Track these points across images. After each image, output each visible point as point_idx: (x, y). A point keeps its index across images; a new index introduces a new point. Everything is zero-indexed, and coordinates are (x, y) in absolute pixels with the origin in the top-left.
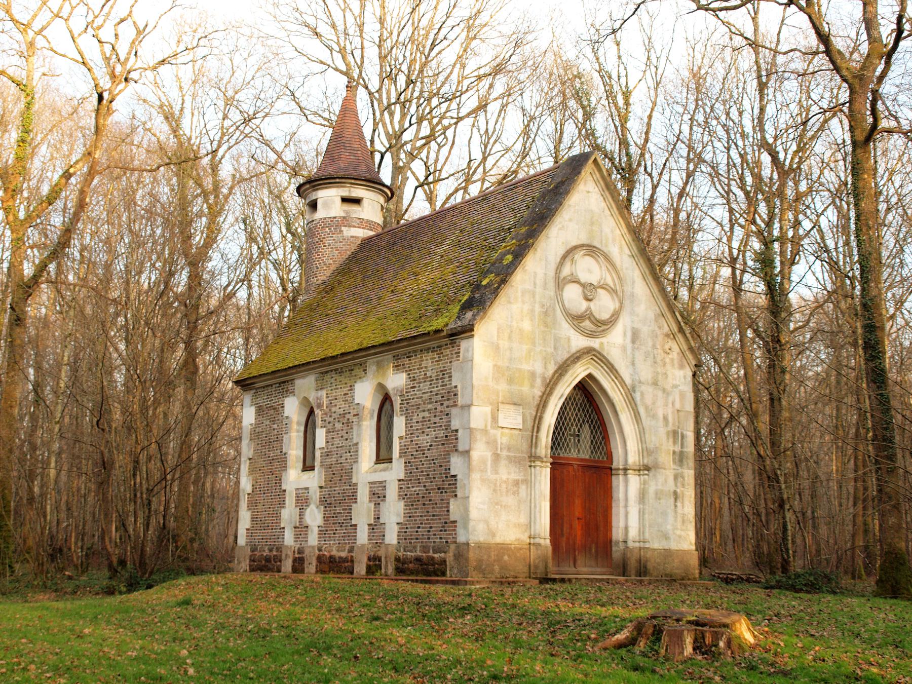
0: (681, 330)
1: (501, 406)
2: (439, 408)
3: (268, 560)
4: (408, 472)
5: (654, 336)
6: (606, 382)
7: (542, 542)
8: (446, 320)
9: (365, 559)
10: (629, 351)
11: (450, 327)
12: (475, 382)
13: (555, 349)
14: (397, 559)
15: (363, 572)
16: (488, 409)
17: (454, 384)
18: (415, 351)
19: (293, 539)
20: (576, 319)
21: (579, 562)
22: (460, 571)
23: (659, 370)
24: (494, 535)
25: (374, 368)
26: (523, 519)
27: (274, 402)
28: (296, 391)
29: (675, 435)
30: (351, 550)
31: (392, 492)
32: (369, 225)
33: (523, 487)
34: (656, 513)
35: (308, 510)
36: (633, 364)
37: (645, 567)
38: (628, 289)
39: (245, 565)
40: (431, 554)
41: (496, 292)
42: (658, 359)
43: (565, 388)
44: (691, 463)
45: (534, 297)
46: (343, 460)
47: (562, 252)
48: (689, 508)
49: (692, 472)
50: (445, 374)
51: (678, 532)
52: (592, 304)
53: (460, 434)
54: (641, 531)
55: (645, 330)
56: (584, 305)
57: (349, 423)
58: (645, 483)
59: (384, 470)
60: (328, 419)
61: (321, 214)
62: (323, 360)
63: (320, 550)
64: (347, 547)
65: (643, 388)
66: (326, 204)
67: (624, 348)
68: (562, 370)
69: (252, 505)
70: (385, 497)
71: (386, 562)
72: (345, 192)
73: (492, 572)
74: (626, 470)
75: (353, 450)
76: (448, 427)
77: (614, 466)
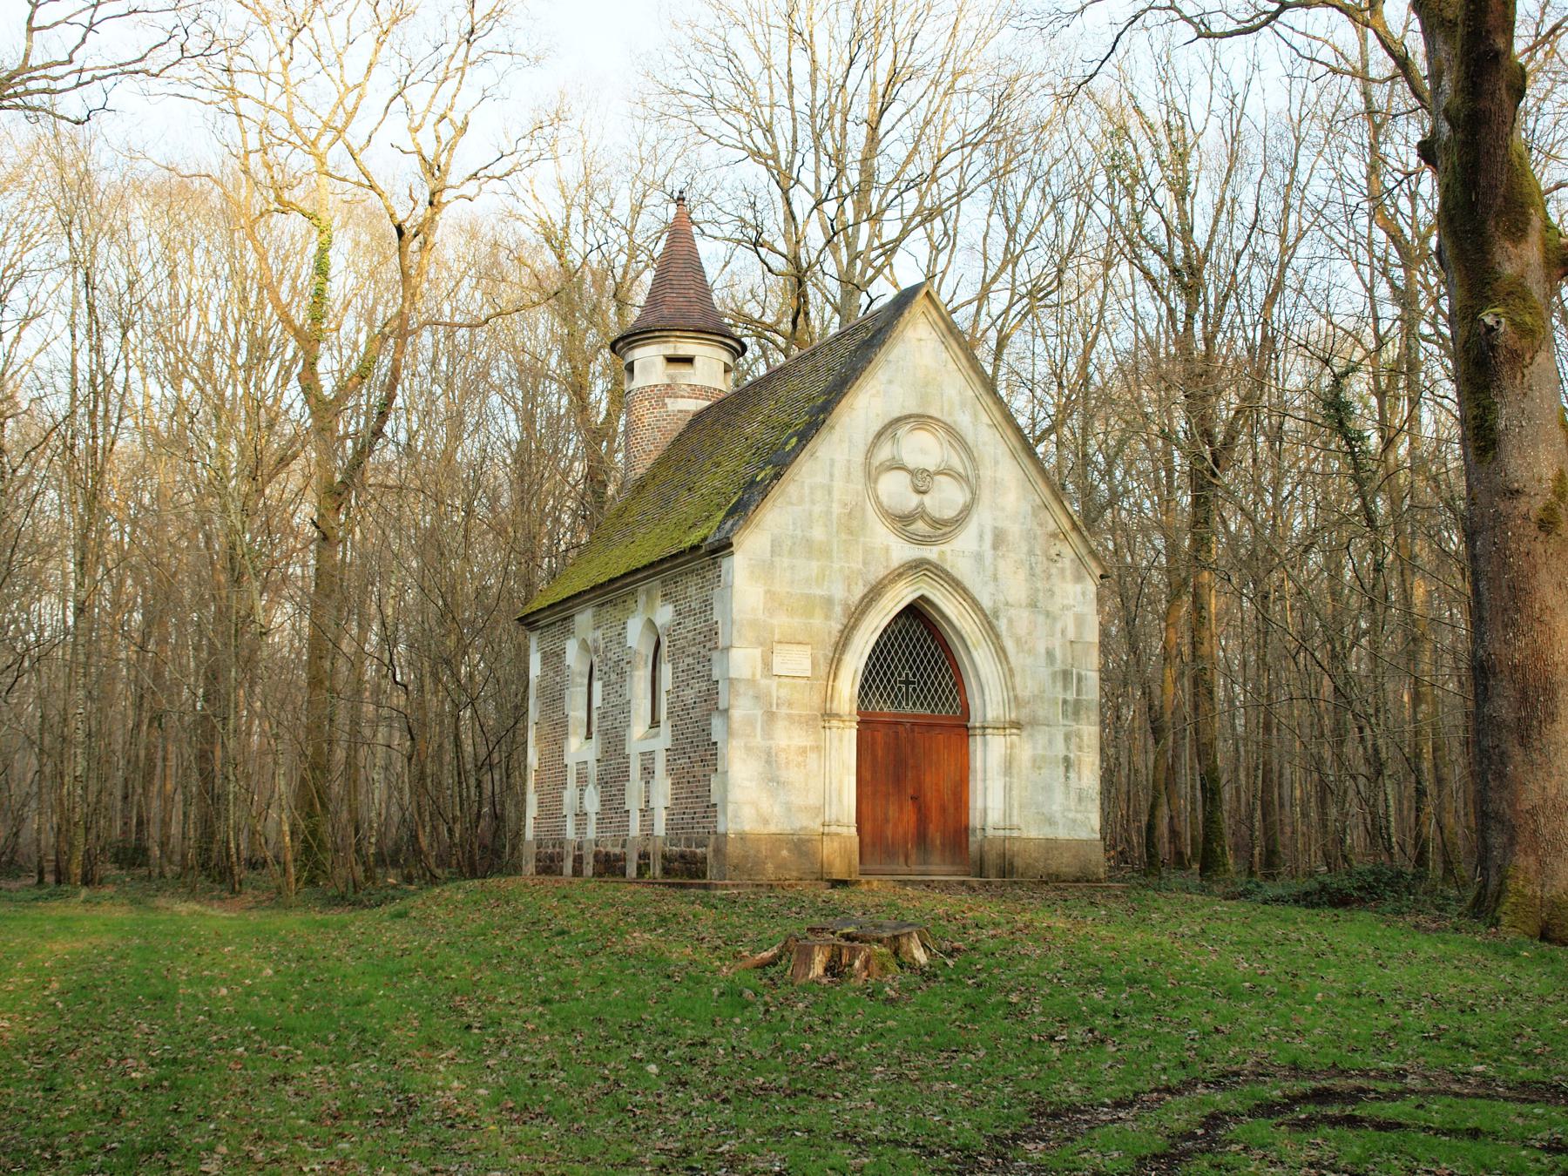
1: (777, 648)
4: (676, 739)
5: (1030, 537)
6: (949, 606)
7: (844, 831)
9: (635, 857)
12: (736, 616)
13: (865, 563)
14: (664, 856)
15: (634, 875)
16: (757, 652)
20: (902, 521)
21: (913, 857)
23: (1039, 585)
24: (766, 822)
33: (814, 756)
36: (995, 579)
37: (1011, 864)
38: (986, 473)
39: (529, 867)
42: (1038, 570)
44: (1095, 717)
45: (830, 493)
47: (877, 427)
50: (707, 604)
51: (1071, 815)
52: (927, 499)
54: (1007, 813)
55: (1014, 530)
57: (622, 674)
61: (639, 381)
62: (593, 589)
65: (1012, 611)
67: (979, 557)
68: (874, 593)
72: (670, 349)
75: (625, 709)
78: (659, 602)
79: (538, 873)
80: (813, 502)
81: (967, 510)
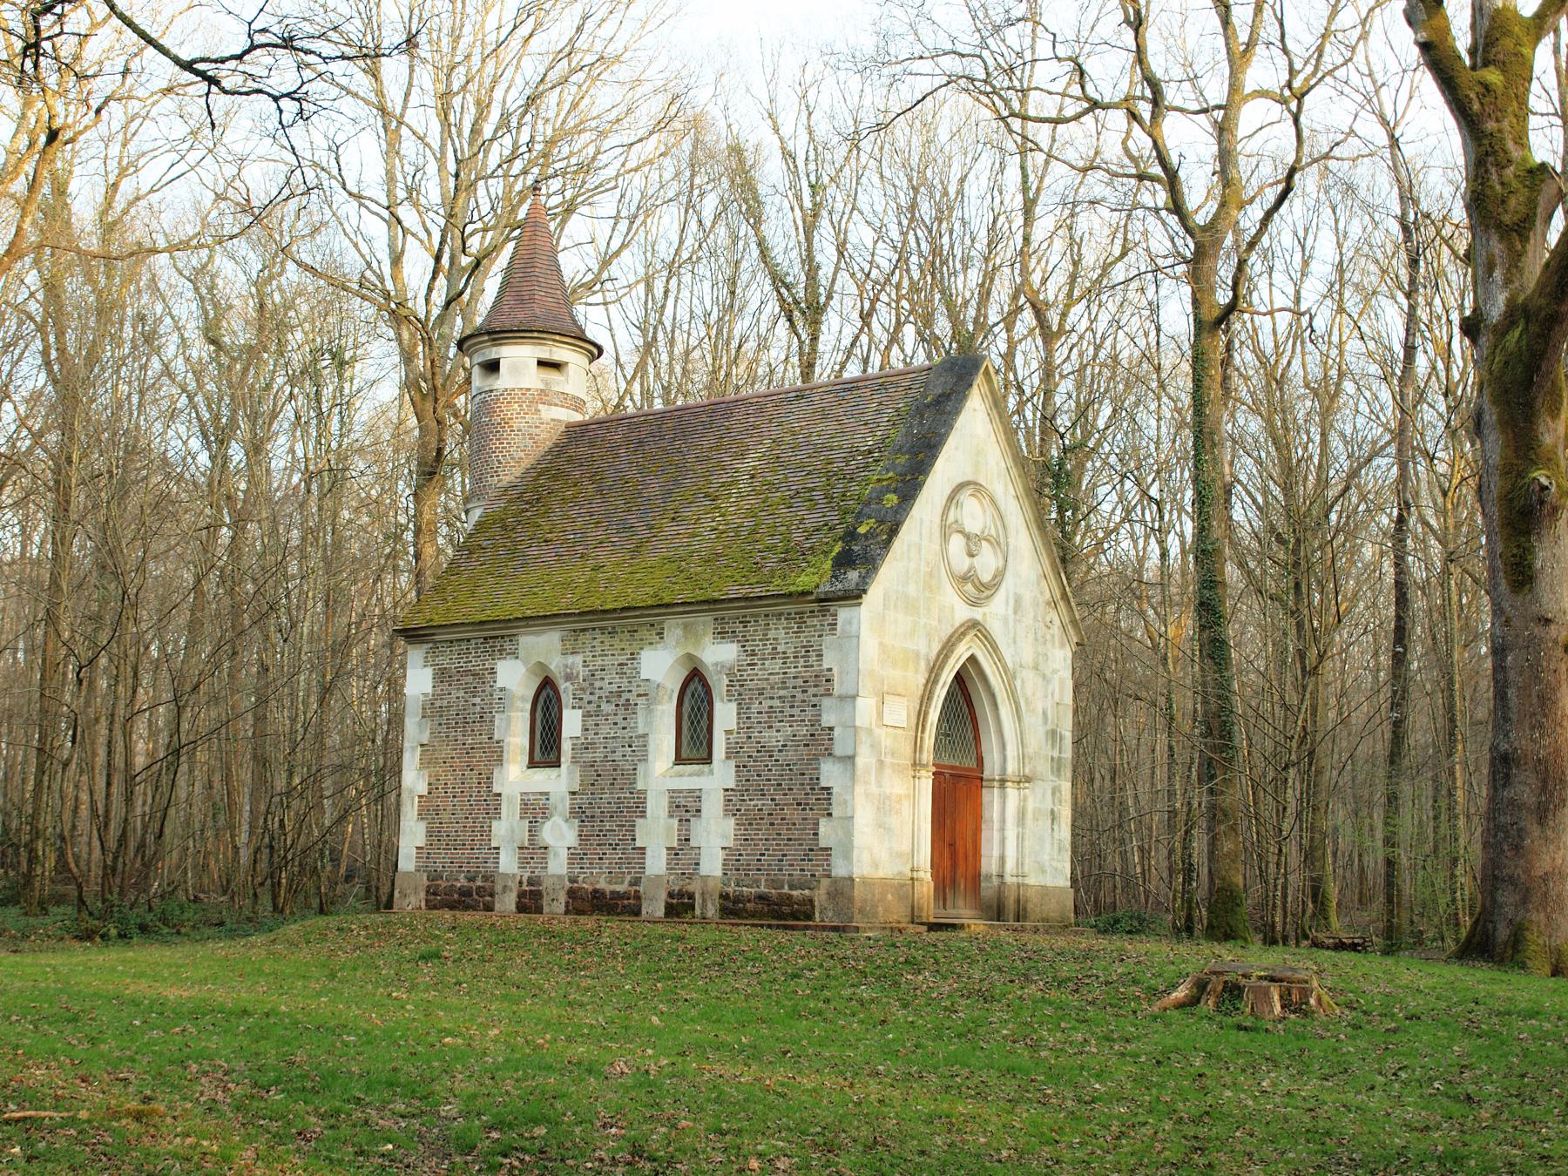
0: (1064, 596)
2: (800, 696)
3: (465, 893)
8: (816, 578)
9: (663, 896)
10: (1011, 624)
15: (660, 912)
17: (825, 666)
18: (752, 616)
19: (516, 865)
22: (837, 914)
24: (877, 867)
25: (679, 632)
26: (905, 847)
27: (475, 663)
28: (522, 653)
29: (1053, 735)
30: (636, 882)
31: (713, 805)
32: (578, 405)
34: (1030, 842)
35: (548, 825)
37: (1025, 909)
38: (1011, 541)
40: (786, 890)
41: (887, 544)
43: (947, 676)
44: (1069, 774)
46: (618, 756)
48: (1065, 832)
49: (1069, 784)
50: (810, 651)
52: (975, 560)
53: (836, 733)
54: (1020, 863)
55: (1027, 597)
56: (967, 561)
58: (1025, 800)
59: (698, 775)
60: (587, 697)
61: (504, 381)
63: (573, 880)
64: (628, 878)
66: (516, 370)
67: (1005, 620)
71: (704, 901)
73: (875, 915)
74: (1003, 782)
75: (639, 747)
76: (815, 722)
77: (986, 774)
78: (709, 638)
79: (431, 906)
81: (1000, 575)
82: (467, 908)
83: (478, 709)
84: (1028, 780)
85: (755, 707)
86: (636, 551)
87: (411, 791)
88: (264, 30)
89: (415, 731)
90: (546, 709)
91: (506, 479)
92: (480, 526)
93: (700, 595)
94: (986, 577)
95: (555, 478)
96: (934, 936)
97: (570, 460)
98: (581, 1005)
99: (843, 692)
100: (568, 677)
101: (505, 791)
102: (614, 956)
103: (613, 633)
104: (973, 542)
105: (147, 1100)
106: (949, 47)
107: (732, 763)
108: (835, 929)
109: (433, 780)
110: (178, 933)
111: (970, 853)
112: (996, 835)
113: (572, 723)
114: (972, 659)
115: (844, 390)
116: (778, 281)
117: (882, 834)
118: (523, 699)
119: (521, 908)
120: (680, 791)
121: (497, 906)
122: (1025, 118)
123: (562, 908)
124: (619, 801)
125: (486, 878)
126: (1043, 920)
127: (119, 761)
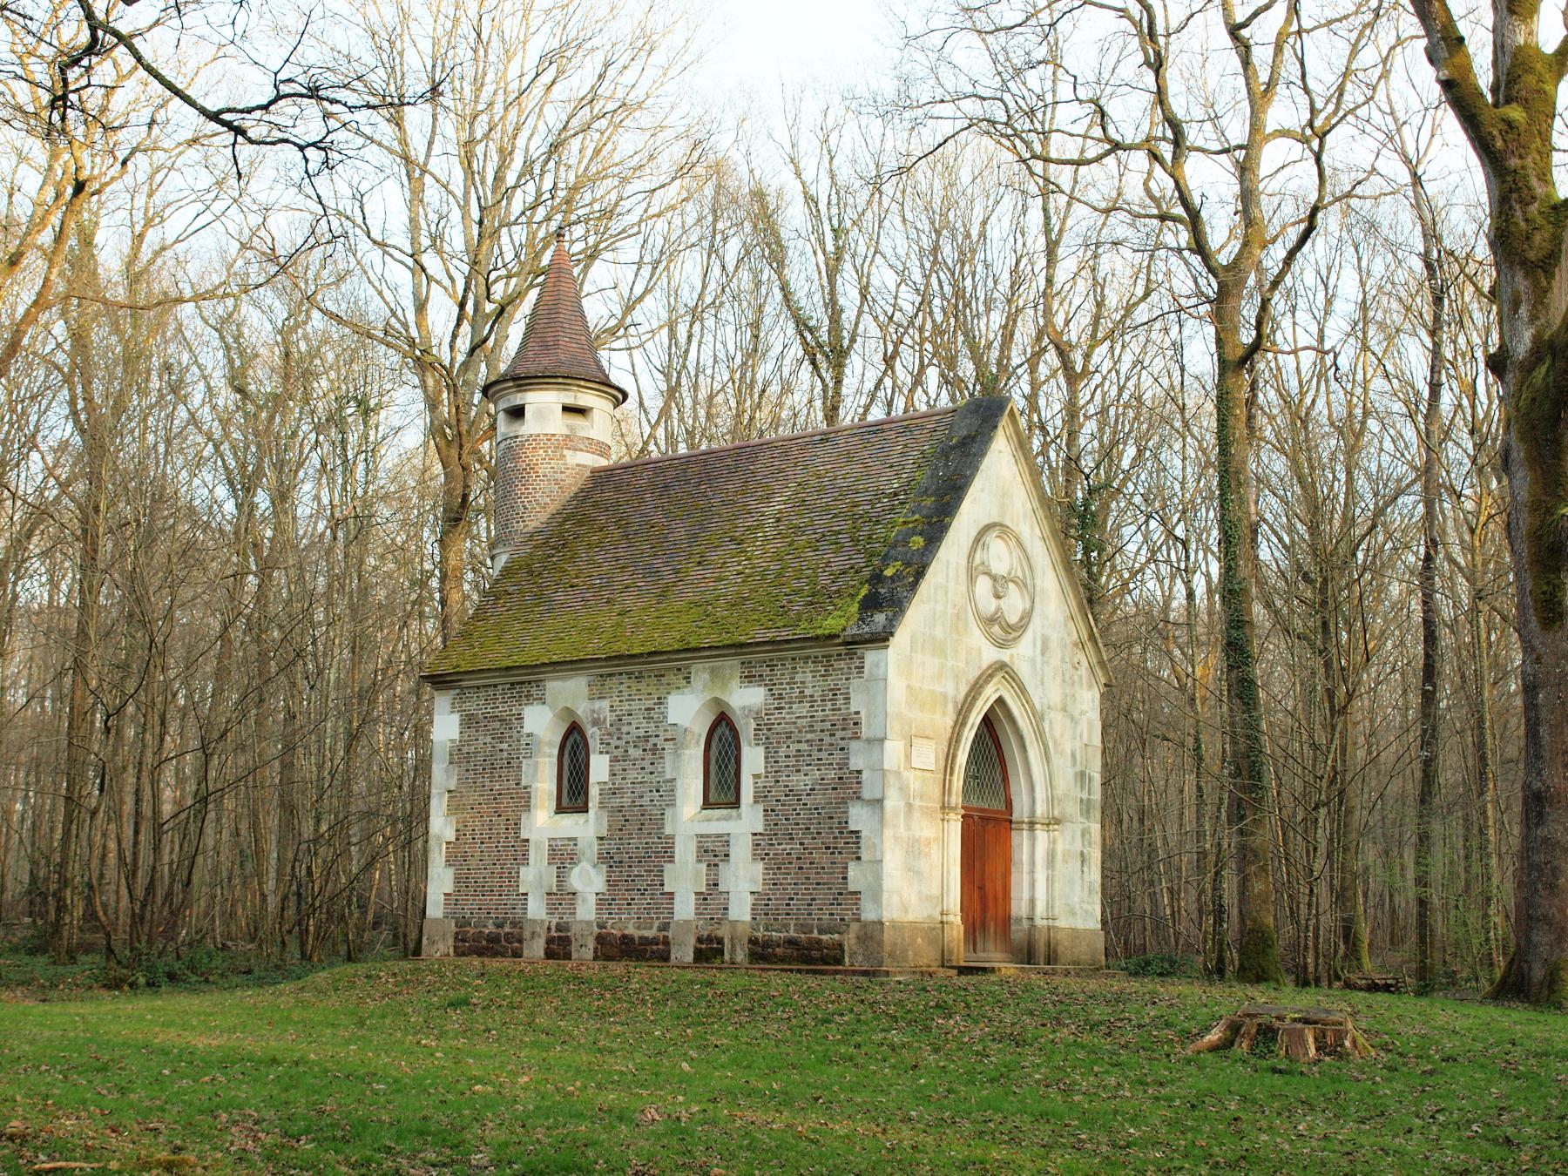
0: (1092, 636)
2: (827, 739)
3: (493, 939)
8: (843, 621)
9: (692, 941)
11: (849, 632)
14: (753, 941)
15: (689, 957)
17: (853, 709)
18: (780, 659)
19: (544, 911)
21: (979, 946)
22: (867, 958)
24: (906, 911)
25: (706, 676)
26: (935, 891)
27: (502, 709)
28: (548, 696)
29: (1082, 777)
30: (664, 927)
31: (741, 850)
32: (603, 450)
34: (1060, 884)
35: (576, 870)
37: (1055, 952)
38: (1038, 582)
40: (815, 934)
43: (975, 718)
44: (1098, 816)
46: (645, 801)
47: (974, 534)
48: (1095, 875)
50: (837, 694)
52: (1002, 602)
53: (864, 776)
54: (1050, 905)
55: (1055, 638)
58: (1054, 842)
60: (614, 742)
61: (529, 427)
63: (601, 926)
66: (540, 415)
67: (1033, 661)
68: (976, 689)
69: (456, 857)
70: (727, 855)
71: (733, 946)
72: (569, 398)
73: (905, 959)
74: (1032, 824)
75: (667, 792)
76: (843, 765)
77: (1015, 817)
78: (736, 682)
79: (459, 953)
80: (936, 602)
81: (1027, 617)
82: (495, 954)
83: (505, 754)
84: (1058, 822)
85: (783, 751)
86: (663, 595)
87: (439, 838)
88: (290, 80)
89: (442, 777)
90: (574, 754)
91: (532, 525)
92: (507, 572)
93: (727, 639)
94: (1013, 619)
95: (580, 523)
96: (964, 979)
97: (595, 505)
98: (611, 1052)
99: (871, 735)
100: (596, 722)
101: (533, 837)
102: (644, 1002)
103: (639, 678)
104: (999, 584)
105: (177, 1150)
106: (969, 89)
107: (761, 807)
108: (865, 973)
109: (460, 826)
110: (207, 981)
111: (1000, 896)
112: (1026, 877)
113: (599, 768)
114: (1000, 701)
115: (869, 433)
116: (802, 325)
117: (911, 876)
118: (550, 744)
119: (550, 954)
120: (708, 836)
121: (526, 953)
122: (1047, 160)
123: (591, 954)
124: (647, 846)
125: (514, 924)
126: (1074, 963)
127: (147, 810)
